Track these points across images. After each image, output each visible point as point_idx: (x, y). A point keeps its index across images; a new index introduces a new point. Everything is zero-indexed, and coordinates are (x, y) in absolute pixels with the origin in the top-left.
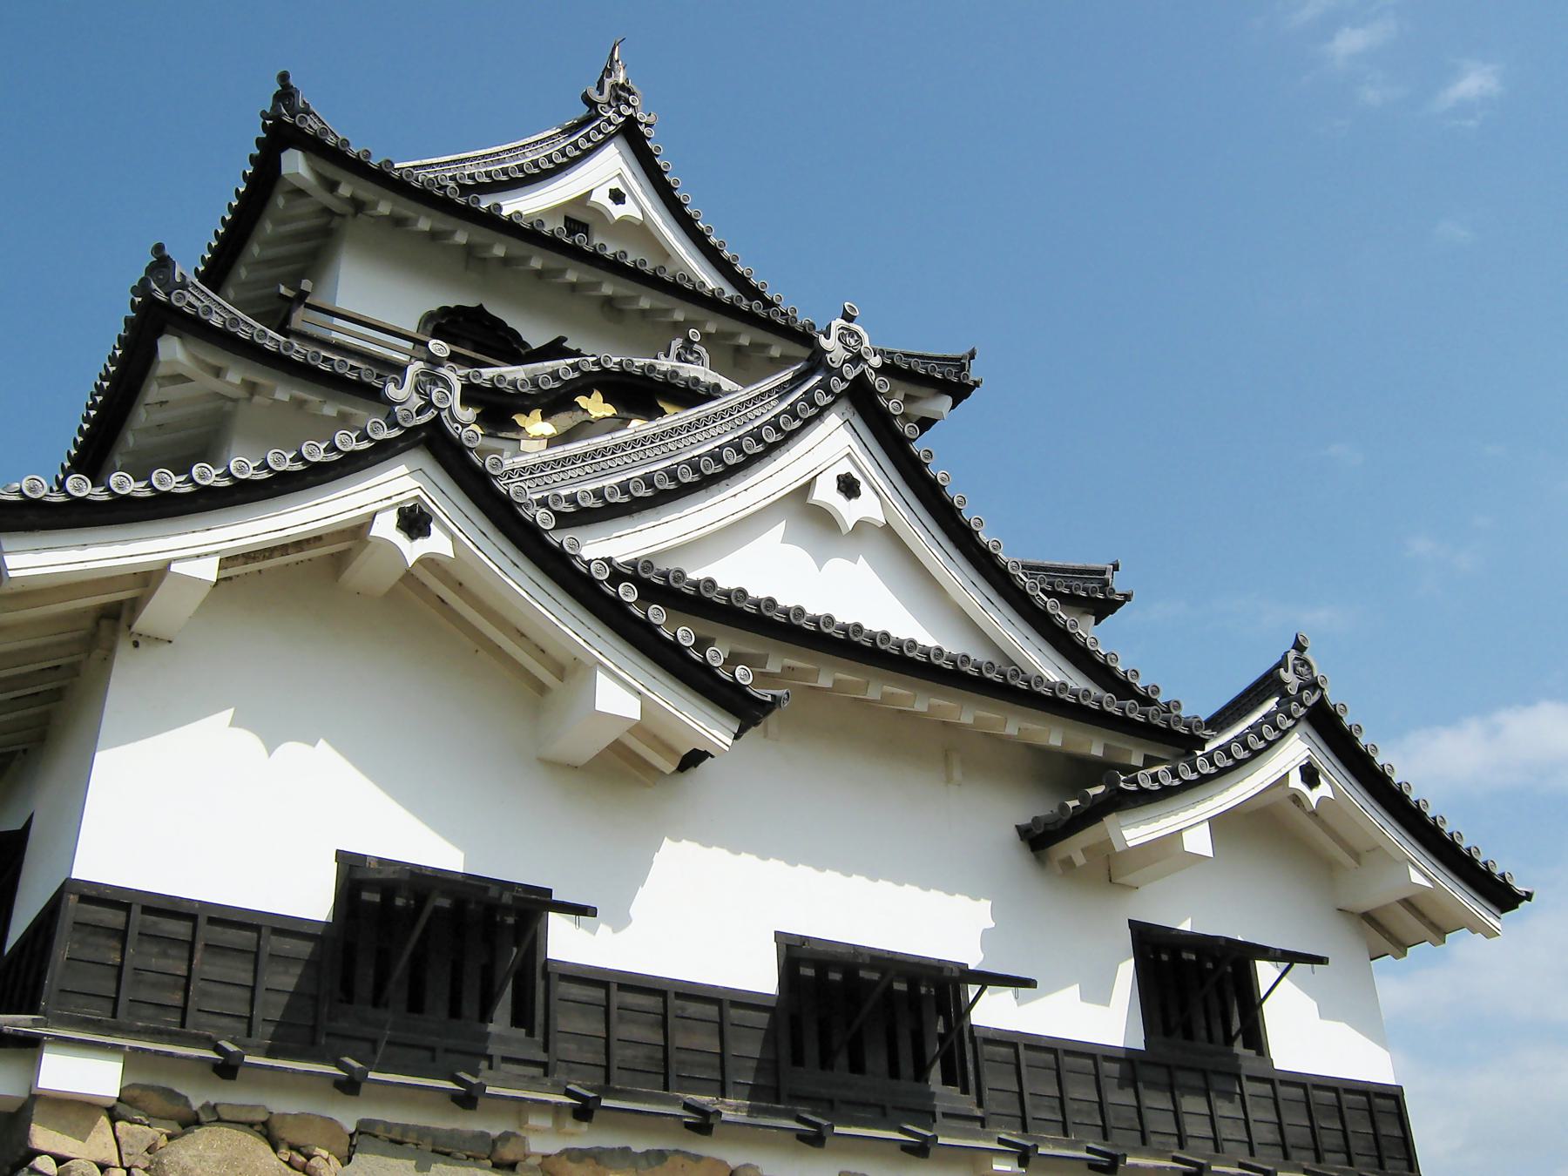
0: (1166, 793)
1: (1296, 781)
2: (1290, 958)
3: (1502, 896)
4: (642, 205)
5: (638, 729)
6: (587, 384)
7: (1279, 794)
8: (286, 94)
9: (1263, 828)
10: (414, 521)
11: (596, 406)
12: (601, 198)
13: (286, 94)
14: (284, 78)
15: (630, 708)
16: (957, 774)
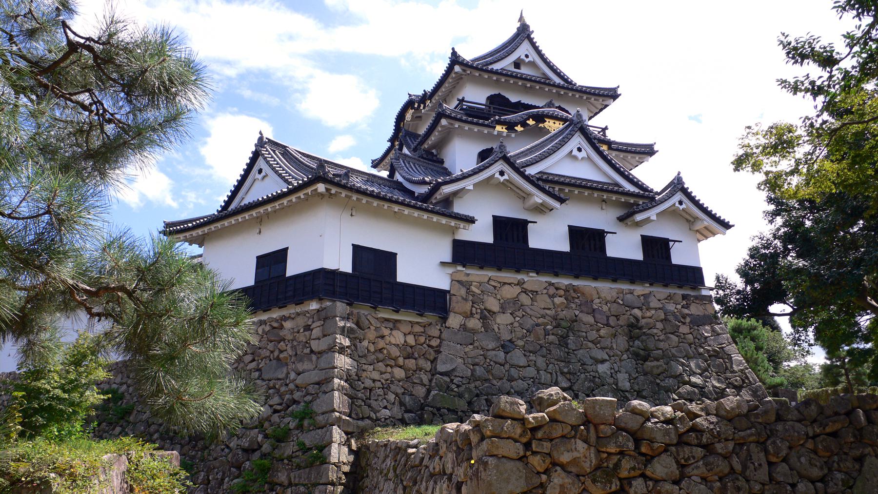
0: (650, 208)
1: (677, 205)
2: (675, 241)
3: (726, 226)
5: (541, 204)
7: (673, 208)
8: (454, 53)
9: (672, 213)
10: (502, 173)
12: (523, 57)
13: (454, 53)
14: (453, 49)
15: (541, 201)
16: (604, 207)
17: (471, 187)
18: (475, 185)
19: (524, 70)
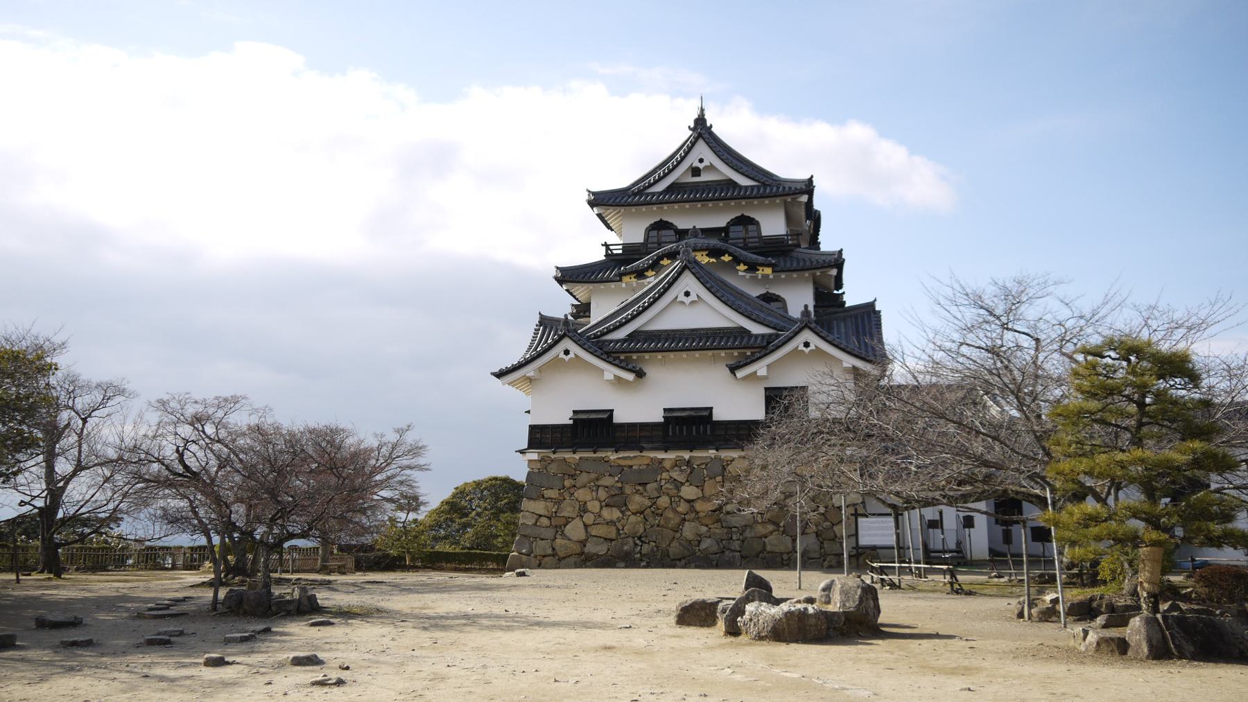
4: (710, 158)
6: (661, 258)
11: (665, 262)
12: (697, 164)
17: (531, 374)
18: (540, 370)
19: (704, 177)
